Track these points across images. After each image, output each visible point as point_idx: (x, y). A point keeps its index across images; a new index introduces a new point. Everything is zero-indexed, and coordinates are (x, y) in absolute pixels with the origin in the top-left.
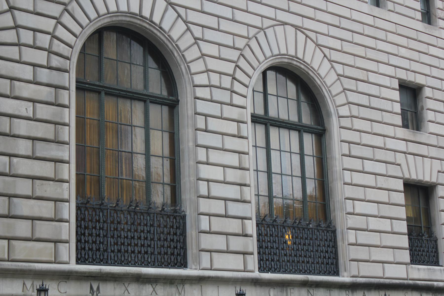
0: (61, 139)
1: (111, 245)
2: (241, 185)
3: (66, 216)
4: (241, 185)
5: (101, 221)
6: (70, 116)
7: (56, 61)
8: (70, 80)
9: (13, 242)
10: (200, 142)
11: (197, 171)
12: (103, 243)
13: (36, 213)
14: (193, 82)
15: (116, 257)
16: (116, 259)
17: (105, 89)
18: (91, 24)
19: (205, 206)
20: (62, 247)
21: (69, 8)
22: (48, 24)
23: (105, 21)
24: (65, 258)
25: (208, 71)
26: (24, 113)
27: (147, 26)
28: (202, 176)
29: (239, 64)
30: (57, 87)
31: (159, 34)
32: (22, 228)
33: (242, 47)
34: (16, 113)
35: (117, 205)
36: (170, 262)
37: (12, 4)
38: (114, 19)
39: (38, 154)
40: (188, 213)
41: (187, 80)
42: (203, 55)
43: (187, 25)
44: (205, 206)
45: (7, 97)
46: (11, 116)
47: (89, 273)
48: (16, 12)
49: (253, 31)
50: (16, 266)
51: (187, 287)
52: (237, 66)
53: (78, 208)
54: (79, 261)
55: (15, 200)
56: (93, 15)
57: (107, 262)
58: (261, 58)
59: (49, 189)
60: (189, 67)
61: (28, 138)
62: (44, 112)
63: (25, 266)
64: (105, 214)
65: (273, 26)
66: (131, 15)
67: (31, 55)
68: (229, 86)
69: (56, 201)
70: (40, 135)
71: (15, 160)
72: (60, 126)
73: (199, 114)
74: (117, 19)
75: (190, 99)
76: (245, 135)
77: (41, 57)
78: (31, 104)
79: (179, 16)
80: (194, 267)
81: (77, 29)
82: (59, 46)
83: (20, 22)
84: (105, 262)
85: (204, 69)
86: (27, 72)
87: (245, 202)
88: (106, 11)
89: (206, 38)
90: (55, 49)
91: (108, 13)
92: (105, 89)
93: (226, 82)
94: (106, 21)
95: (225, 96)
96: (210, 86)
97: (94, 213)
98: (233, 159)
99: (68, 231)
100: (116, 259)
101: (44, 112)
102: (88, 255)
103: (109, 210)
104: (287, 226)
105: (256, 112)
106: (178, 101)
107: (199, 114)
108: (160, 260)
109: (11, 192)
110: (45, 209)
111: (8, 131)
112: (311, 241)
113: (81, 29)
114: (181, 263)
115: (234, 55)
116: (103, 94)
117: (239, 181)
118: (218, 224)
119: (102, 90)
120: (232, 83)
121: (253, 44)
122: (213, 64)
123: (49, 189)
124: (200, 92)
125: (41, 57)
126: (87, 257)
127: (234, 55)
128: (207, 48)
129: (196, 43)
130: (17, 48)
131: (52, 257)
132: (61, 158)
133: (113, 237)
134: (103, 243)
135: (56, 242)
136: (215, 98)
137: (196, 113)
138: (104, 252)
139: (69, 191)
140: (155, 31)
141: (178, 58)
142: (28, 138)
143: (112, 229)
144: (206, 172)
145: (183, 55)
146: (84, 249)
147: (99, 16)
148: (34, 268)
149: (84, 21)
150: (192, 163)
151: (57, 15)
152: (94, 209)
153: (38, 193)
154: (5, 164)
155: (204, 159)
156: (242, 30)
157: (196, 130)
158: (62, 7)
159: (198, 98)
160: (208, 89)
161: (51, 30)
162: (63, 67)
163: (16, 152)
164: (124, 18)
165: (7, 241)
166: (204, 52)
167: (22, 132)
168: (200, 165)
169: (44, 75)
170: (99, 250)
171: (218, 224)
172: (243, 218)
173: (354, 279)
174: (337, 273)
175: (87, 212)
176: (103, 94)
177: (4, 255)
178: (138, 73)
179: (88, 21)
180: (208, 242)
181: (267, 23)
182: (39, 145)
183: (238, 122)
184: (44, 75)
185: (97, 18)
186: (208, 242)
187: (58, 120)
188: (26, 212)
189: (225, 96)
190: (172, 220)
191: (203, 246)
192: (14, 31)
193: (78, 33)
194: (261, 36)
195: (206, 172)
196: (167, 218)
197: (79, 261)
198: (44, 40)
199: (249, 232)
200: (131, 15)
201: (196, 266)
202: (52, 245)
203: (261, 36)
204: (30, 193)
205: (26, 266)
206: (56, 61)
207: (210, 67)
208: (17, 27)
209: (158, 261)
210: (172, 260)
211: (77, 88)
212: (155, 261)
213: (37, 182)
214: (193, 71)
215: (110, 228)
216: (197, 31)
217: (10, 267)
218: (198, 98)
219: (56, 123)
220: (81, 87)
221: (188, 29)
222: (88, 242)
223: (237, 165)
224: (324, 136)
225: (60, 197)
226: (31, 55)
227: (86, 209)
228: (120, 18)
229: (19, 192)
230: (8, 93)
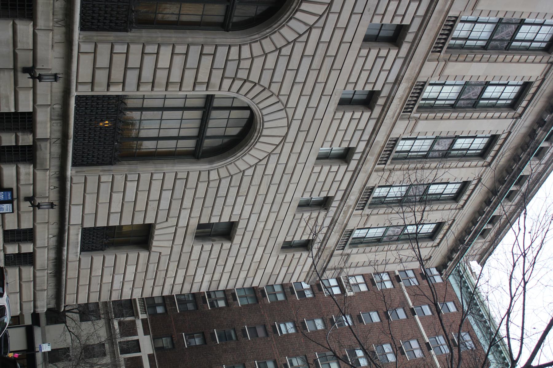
2: (153, 83)
4: (153, 83)
10: (191, 48)
11: (167, 44)
14: (244, 44)
19: (136, 49)
25: (253, 58)
27: (293, 7)
28: (162, 49)
29: (257, 86)
31: (286, 16)
33: (271, 89)
40: (129, 34)
41: (246, 39)
42: (266, 55)
43: (292, 42)
44: (136, 49)
49: (284, 99)
51: (63, 29)
52: (255, 84)
58: (261, 106)
60: (257, 41)
65: (287, 117)
68: (238, 76)
73: (216, 49)
75: (229, 41)
76: (197, 89)
79: (300, 35)
80: (81, 37)
85: (254, 55)
87: (138, 86)
89: (280, 58)
93: (242, 74)
95: (230, 72)
96: (240, 59)
98: (175, 77)
105: (215, 99)
106: (228, 31)
107: (216, 49)
115: (265, 82)
117: (156, 81)
118: (119, 60)
120: (241, 79)
121: (273, 99)
122: (258, 63)
124: (234, 50)
127: (265, 82)
128: (271, 59)
129: (277, 49)
136: (229, 63)
137: (216, 46)
140: (288, 14)
141: (265, 33)
144: (165, 52)
145: (267, 37)
150: (173, 40)
155: (176, 51)
157: (203, 46)
159: (229, 49)
160: (237, 57)
166: (269, 56)
168: (171, 47)
171: (119, 60)
172: (124, 83)
180: (104, 50)
181: (290, 112)
183: (208, 83)
186: (104, 50)
189: (230, 72)
190: (123, 19)
191: (100, 46)
194: (279, 106)
195: (165, 52)
199: (112, 89)
201: (82, 38)
203: (279, 106)
207: (255, 60)
209: (86, 4)
210: (88, 18)
214: (253, 45)
216: (286, 51)
218: (229, 49)
221: (289, 43)
223: (171, 80)
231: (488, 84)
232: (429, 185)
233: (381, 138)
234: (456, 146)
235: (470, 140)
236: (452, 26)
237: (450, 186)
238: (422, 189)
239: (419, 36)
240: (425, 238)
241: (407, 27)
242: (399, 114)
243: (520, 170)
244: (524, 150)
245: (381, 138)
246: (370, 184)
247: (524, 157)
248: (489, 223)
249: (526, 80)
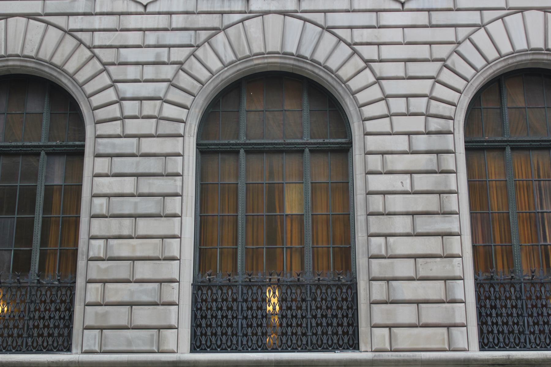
0: (447, 209)
1: (528, 325)
3: (459, 296)
5: (513, 297)
6: (460, 182)
7: (435, 124)
8: (458, 141)
9: (394, 330)
12: (517, 324)
13: (421, 296)
15: (538, 339)
16: (538, 342)
17: (510, 144)
18: (479, 74)
20: (170, 334)
21: (449, 63)
22: (424, 86)
23: (499, 67)
24: (172, 346)
26: (399, 188)
30: (438, 152)
32: (405, 314)
34: (390, 189)
35: (533, 276)
36: (211, 345)
37: (378, 75)
38: (510, 61)
39: (419, 230)
45: (380, 173)
46: (384, 193)
47: (493, 360)
48: (383, 82)
50: (397, 356)
53: (478, 285)
54: (483, 347)
55: (394, 283)
56: (479, 63)
57: (525, 347)
59: (436, 268)
61: (407, 214)
62: (423, 182)
63: (408, 356)
64: (518, 289)
66: (533, 52)
67: (402, 124)
69: (445, 279)
70: (420, 209)
71: (391, 240)
72: (445, 195)
74: (515, 60)
77: (417, 124)
78: (408, 176)
81: (459, 83)
82: (438, 106)
83: (388, 92)
84: (522, 346)
86: (401, 143)
88: (497, 55)
90: (433, 111)
91: (501, 57)
92: (510, 144)
94: (499, 66)
97: (502, 289)
99: (467, 312)
100: (538, 342)
101: (423, 182)
102: (498, 339)
103: (523, 285)
104: (498, 284)
108: (533, 340)
109: (389, 275)
110: (434, 290)
111: (381, 210)
112: (519, 302)
113: (465, 82)
114: (339, 345)
115: (431, 69)
116: (508, 150)
119: (507, 145)
123: (436, 268)
125: (417, 124)
126: (496, 341)
130: (388, 119)
131: (444, 344)
132: (448, 231)
133: (531, 316)
134: (517, 324)
135: (448, 326)
138: (18, 338)
139: (465, 266)
142: (407, 214)
143: (530, 306)
146: (492, 332)
147: (489, 63)
148: (420, 358)
149: (469, 72)
151: (434, 74)
152: (502, 285)
153: (422, 273)
154: (380, 246)
156: (448, 34)
158: (440, 64)
161: (427, 92)
162: (445, 129)
163: (392, 231)
164: (524, 58)
165: (387, 329)
167: (398, 209)
169: (421, 143)
170: (512, 332)
173: (377, 354)
174: (355, 347)
175: (492, 289)
176: (508, 150)
177: (385, 345)
178: (292, 121)
179: (474, 71)
182: (419, 219)
184: (421, 143)
185: (486, 66)
187: (442, 188)
188: (408, 296)
192: (383, 102)
193: (461, 88)
196: (510, 287)
197: (483, 347)
198: (419, 105)
200: (533, 52)
202: (444, 330)
204: (412, 274)
205: (410, 356)
206: (435, 124)
208: (386, 97)
209: (530, 342)
211: (468, 149)
212: (526, 342)
213: (420, 261)
215: (311, 307)
217: (390, 358)
219: (440, 193)
220: (471, 148)
222: (497, 324)
224: (351, 151)
225: (451, 275)
226: (402, 124)
227: (492, 285)
228: (519, 59)
229: (398, 274)
230: (380, 169)
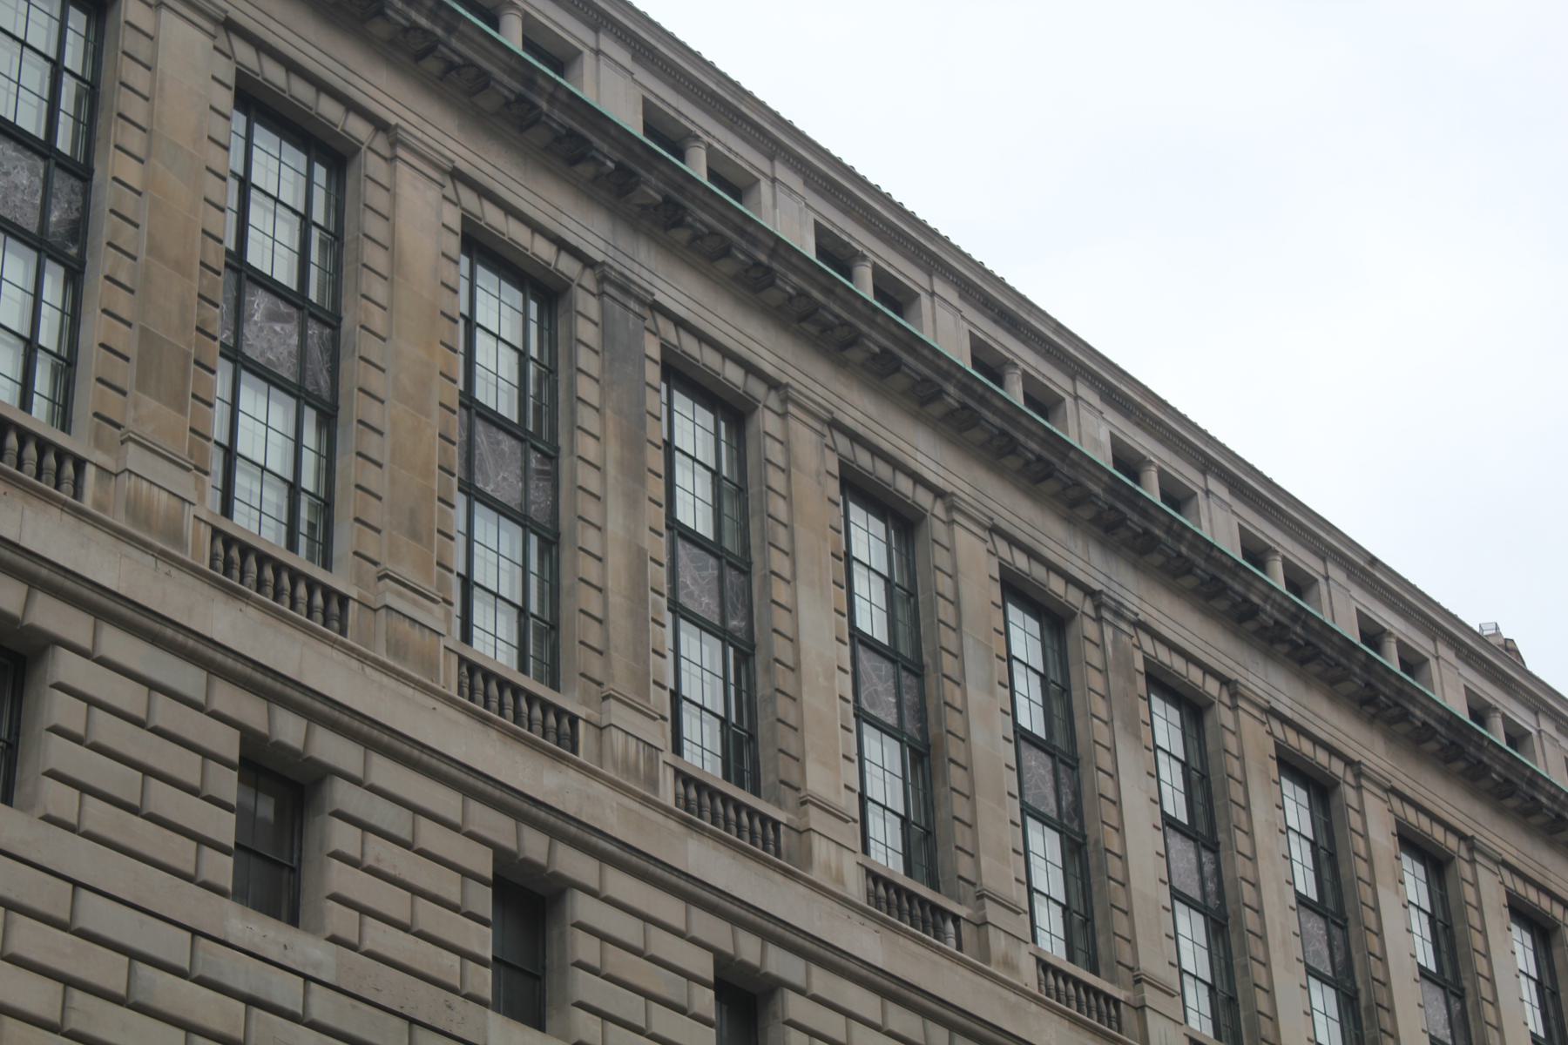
231: (468, 400)
232: (859, 639)
233: (867, 942)
234: (705, 528)
235: (859, 574)
236: (246, 549)
237: (859, 550)
238: (1178, 843)
239: (326, 709)
240: (1326, 810)
241: (723, 962)
242: (581, 768)
243: (948, 369)
244: (854, 340)
245: (867, 942)
246: (855, 887)
247: (794, 278)
248: (1136, 478)
249: (833, 488)
